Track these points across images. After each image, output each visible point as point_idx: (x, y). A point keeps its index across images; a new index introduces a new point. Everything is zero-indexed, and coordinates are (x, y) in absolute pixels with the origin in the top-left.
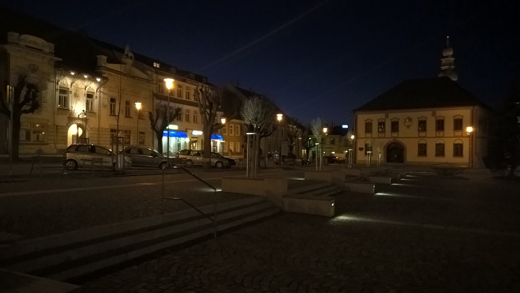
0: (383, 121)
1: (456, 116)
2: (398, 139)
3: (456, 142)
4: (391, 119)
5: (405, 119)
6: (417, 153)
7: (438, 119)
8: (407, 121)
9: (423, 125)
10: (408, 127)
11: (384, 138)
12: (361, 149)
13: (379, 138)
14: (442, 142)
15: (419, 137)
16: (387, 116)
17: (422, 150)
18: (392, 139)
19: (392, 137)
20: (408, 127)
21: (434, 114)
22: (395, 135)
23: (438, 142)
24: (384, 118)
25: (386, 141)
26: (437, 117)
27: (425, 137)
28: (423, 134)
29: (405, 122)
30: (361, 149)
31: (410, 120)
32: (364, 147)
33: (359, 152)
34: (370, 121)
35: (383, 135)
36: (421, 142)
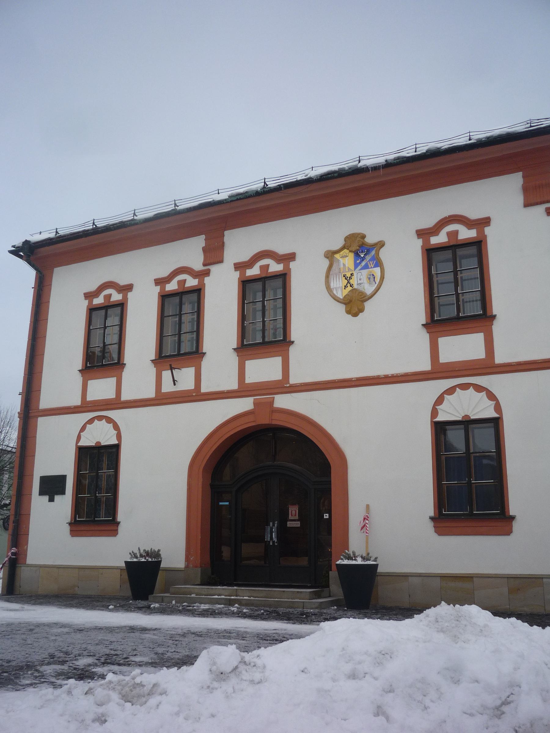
0: (191, 282)
2: (282, 401)
4: (240, 267)
5: (330, 255)
6: (428, 507)
8: (347, 261)
10: (355, 304)
11: (195, 396)
12: (52, 486)
13: (162, 399)
15: (439, 371)
16: (214, 254)
18: (246, 404)
20: (355, 304)
22: (264, 369)
24: (198, 265)
25: (204, 421)
27: (488, 366)
28: (462, 347)
30: (52, 486)
31: (362, 249)
32: (65, 465)
35: (185, 378)
36: (450, 412)
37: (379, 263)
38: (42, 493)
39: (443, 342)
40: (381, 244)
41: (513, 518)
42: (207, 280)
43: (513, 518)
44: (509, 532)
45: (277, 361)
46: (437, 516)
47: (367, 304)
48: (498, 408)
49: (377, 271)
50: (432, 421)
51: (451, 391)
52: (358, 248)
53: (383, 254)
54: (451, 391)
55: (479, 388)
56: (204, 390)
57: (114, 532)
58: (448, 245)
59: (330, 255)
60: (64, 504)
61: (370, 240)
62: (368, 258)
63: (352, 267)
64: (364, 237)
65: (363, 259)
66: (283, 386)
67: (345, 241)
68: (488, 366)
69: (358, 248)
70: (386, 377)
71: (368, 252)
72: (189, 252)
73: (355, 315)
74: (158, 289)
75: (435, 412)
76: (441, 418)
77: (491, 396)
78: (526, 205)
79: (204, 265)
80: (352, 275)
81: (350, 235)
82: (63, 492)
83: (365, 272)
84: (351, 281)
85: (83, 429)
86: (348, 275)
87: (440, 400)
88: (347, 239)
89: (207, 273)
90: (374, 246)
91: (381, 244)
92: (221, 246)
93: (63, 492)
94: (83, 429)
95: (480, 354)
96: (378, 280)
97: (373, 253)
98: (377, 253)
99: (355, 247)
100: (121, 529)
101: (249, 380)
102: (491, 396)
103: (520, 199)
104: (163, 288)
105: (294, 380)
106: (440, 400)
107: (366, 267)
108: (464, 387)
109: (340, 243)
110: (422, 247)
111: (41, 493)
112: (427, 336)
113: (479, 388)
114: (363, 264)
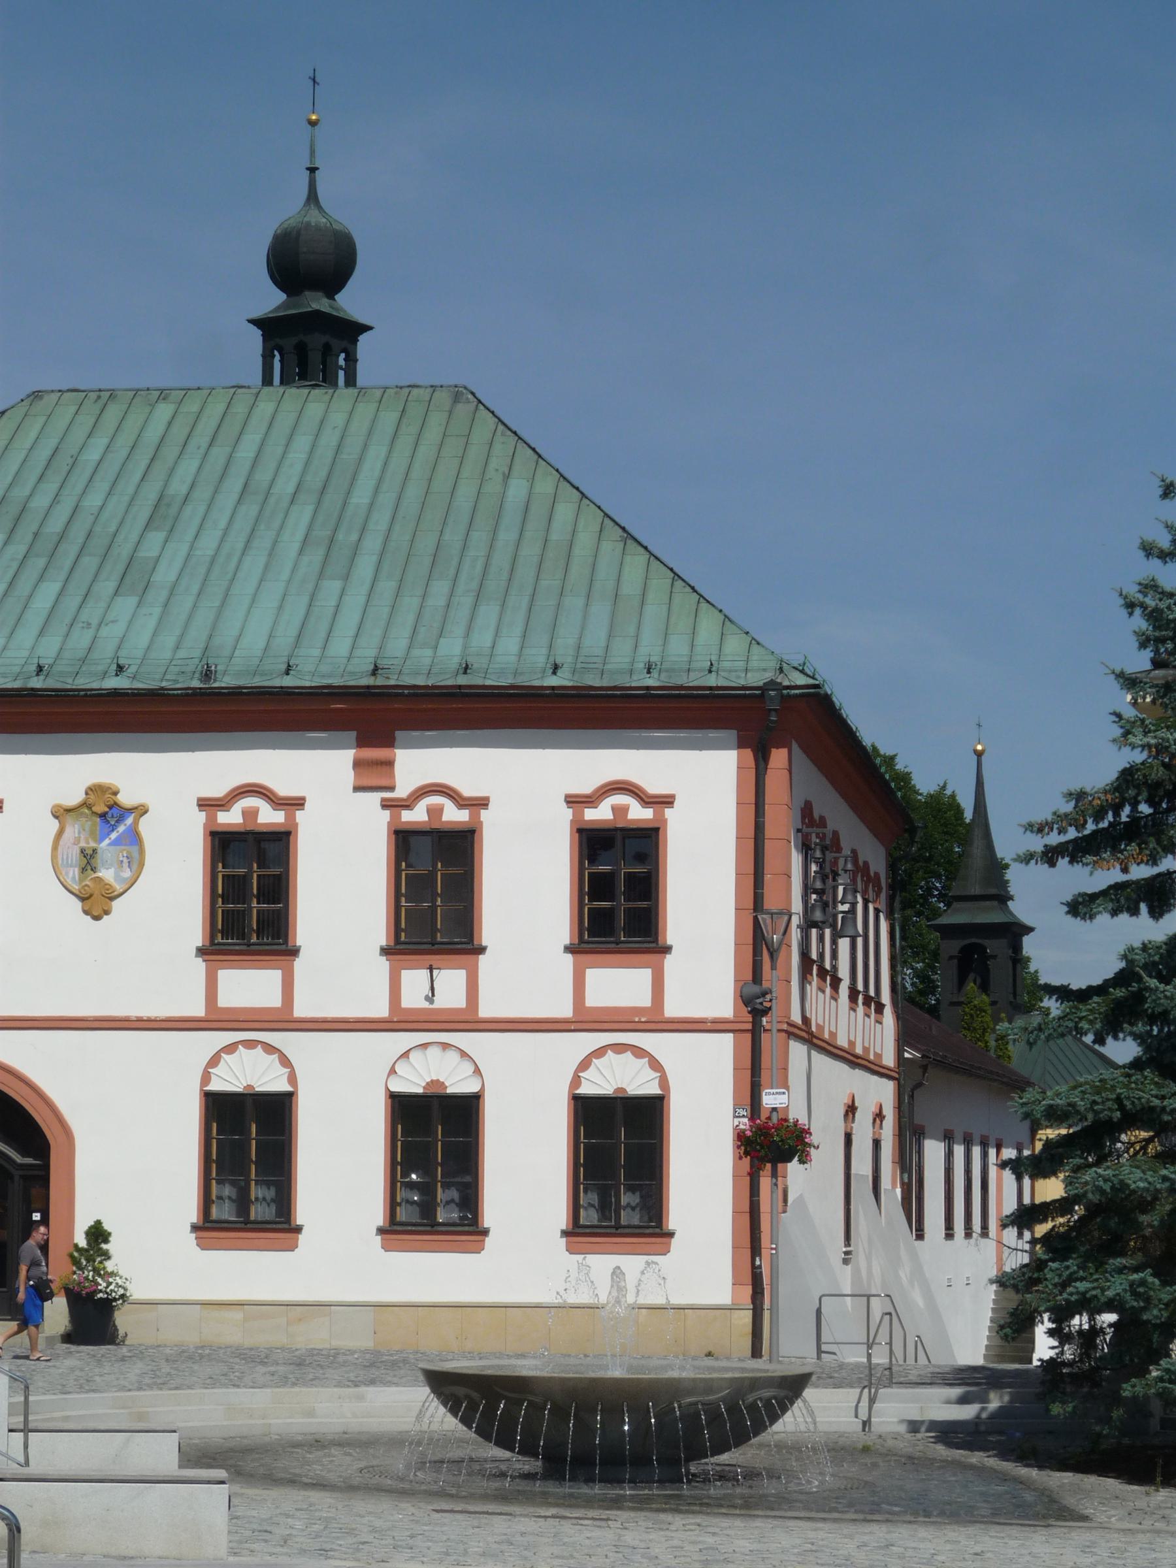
1: (591, 800)
3: (598, 1084)
7: (417, 815)
9: (251, 891)
10: (96, 902)
14: (459, 1083)
15: (216, 1019)
20: (96, 902)
23: (412, 1082)
26: (407, 804)
27: (282, 1020)
28: (250, 986)
40: (141, 810)
44: (292, 1247)
46: (201, 1224)
48: (292, 1078)
50: (201, 1090)
51: (231, 1048)
52: (107, 809)
54: (231, 1048)
55: (270, 1049)
58: (242, 830)
59: (61, 813)
61: (126, 799)
62: (121, 828)
64: (116, 793)
67: (87, 794)
68: (282, 1020)
69: (107, 809)
70: (140, 1020)
71: (120, 820)
73: (97, 918)
75: (206, 1078)
76: (215, 1086)
77: (285, 1061)
78: (357, 789)
80: (95, 851)
81: (94, 785)
84: (93, 861)
86: (90, 852)
87: (214, 1061)
88: (90, 790)
90: (130, 810)
91: (141, 810)
97: (129, 821)
98: (136, 822)
102: (285, 1061)
106: (214, 1061)
108: (250, 1044)
109: (75, 797)
110: (205, 826)
113: (270, 1049)
114: (114, 836)
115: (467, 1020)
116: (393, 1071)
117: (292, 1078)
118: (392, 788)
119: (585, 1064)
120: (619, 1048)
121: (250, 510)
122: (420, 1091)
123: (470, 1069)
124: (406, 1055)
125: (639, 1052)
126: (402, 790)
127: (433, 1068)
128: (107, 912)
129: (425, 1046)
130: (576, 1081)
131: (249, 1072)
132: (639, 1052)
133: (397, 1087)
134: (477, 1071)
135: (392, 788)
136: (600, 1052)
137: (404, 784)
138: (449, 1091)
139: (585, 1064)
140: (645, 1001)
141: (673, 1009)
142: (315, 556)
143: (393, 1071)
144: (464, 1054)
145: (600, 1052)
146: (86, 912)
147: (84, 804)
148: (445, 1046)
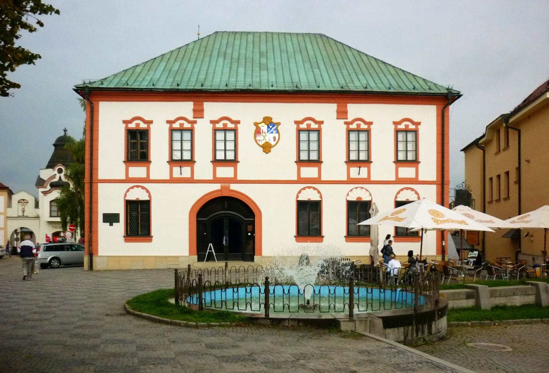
0: (187, 125)
5: (256, 124)
6: (294, 233)
8: (264, 127)
10: (267, 148)
11: (191, 180)
12: (111, 219)
13: (173, 180)
14: (365, 198)
15: (300, 181)
16: (199, 113)
17: (309, 219)
18: (217, 187)
19: (215, 180)
20: (267, 148)
21: (342, 114)
22: (225, 172)
23: (353, 197)
24: (190, 117)
25: (197, 193)
26: (351, 123)
29: (258, 132)
30: (111, 219)
32: (120, 209)
33: (103, 228)
34: (143, 126)
35: (186, 172)
36: (303, 197)
37: (278, 132)
38: (105, 221)
39: (302, 169)
40: (279, 124)
41: (323, 237)
42: (195, 125)
43: (323, 237)
45: (232, 169)
47: (272, 149)
48: (321, 197)
49: (277, 135)
51: (304, 189)
53: (280, 128)
56: (196, 178)
57: (150, 241)
59: (256, 124)
60: (120, 227)
61: (274, 121)
63: (266, 132)
64: (272, 119)
65: (271, 129)
66: (234, 180)
68: (318, 181)
72: (185, 108)
73: (267, 153)
74: (168, 125)
75: (297, 197)
76: (300, 199)
78: (337, 119)
79: (194, 118)
82: (118, 221)
83: (272, 135)
85: (128, 191)
87: (300, 192)
89: (195, 122)
91: (279, 124)
92: (202, 111)
93: (118, 221)
94: (128, 191)
95: (316, 176)
96: (277, 139)
97: (275, 127)
99: (268, 123)
100: (153, 239)
101: (218, 176)
102: (319, 192)
103: (335, 115)
104: (171, 126)
105: (239, 178)
106: (300, 192)
107: (272, 132)
108: (309, 188)
111: (105, 221)
112: (296, 166)
115: (367, 181)
116: (348, 195)
117: (321, 197)
118: (347, 119)
119: (398, 193)
120: (407, 189)
121: (284, 55)
122: (355, 200)
123: (369, 194)
124: (351, 190)
125: (412, 190)
126: (350, 119)
127: (359, 194)
128: (270, 152)
129: (356, 188)
130: (396, 197)
131: (309, 195)
132: (412, 190)
133: (349, 199)
134: (370, 195)
135: (347, 119)
136: (402, 190)
137: (350, 119)
138: (363, 200)
139: (398, 193)
140: (414, 176)
141: (421, 178)
142: (308, 65)
143: (348, 195)
144: (367, 190)
145: (402, 190)
146: (264, 151)
147: (263, 122)
148: (362, 188)
